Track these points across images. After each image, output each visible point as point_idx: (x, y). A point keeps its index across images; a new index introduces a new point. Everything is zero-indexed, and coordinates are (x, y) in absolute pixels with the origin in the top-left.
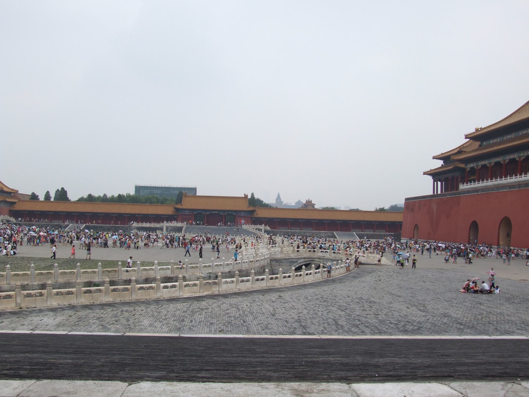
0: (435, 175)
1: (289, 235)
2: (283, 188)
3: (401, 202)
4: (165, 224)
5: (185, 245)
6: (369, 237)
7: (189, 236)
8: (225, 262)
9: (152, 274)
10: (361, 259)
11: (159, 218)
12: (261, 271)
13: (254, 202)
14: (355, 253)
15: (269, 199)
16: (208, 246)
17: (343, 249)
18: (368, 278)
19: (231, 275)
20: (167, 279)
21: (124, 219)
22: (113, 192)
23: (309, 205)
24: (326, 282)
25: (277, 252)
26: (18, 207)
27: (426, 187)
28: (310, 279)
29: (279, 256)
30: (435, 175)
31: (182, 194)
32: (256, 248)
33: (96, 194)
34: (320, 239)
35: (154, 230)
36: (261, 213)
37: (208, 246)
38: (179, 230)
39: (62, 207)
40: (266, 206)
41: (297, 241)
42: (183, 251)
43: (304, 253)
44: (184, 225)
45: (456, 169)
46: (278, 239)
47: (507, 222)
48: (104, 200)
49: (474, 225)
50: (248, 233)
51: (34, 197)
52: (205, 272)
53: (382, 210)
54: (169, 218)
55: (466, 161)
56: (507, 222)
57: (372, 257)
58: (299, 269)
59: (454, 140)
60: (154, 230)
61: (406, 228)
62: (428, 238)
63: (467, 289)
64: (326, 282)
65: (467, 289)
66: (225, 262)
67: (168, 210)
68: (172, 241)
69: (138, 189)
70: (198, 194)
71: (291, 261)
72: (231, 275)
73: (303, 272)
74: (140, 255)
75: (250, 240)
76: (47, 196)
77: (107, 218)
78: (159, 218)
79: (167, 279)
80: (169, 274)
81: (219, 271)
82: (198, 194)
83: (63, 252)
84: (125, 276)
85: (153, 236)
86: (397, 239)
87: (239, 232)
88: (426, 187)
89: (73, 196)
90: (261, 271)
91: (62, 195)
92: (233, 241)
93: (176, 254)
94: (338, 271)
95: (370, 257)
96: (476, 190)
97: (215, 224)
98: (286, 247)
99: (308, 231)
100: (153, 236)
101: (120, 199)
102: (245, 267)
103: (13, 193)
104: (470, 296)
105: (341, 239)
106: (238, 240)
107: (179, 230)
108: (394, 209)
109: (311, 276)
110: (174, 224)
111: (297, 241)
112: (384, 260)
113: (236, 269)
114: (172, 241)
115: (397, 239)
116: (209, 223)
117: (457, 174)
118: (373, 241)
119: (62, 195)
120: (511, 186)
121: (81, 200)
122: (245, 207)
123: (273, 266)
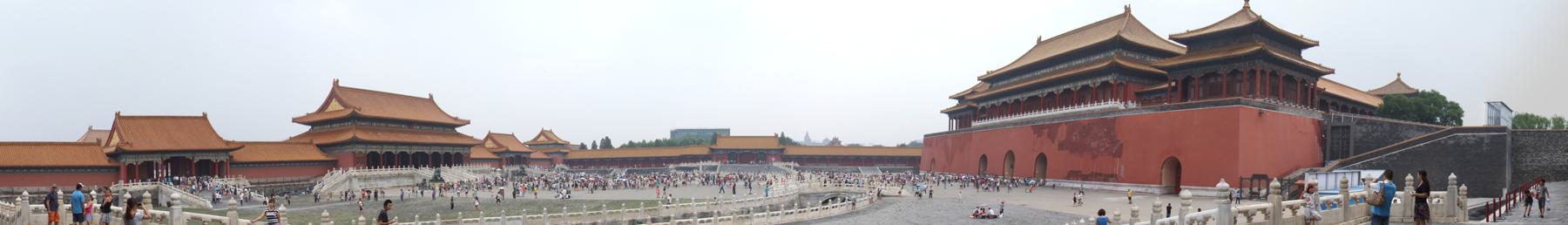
0: (952, 113)
1: (817, 171)
2: (811, 126)
3: (920, 139)
4: (701, 164)
5: (719, 182)
6: (891, 171)
7: (723, 175)
8: (756, 197)
9: (689, 210)
10: (884, 192)
11: (695, 158)
12: (790, 205)
13: (784, 140)
14: (878, 185)
15: (798, 138)
16: (741, 183)
17: (867, 181)
18: (890, 209)
19: (762, 209)
20: (704, 215)
21: (660, 161)
22: (650, 138)
23: (836, 141)
24: (851, 214)
25: (805, 187)
26: (571, 156)
27: (943, 124)
28: (836, 212)
29: (807, 191)
30: (952, 113)
31: (716, 135)
32: (786, 183)
33: (636, 141)
34: (845, 173)
35: (691, 169)
36: (791, 151)
37: (741, 183)
38: (714, 168)
39: (606, 155)
40: (795, 144)
41: (824, 176)
42: (717, 188)
43: (831, 187)
44: (718, 164)
45: (970, 108)
46: (807, 175)
47: (1011, 155)
48: (644, 145)
49: (984, 158)
50: (778, 170)
51: (583, 147)
52: (738, 207)
53: (903, 146)
54: (705, 158)
55: (978, 101)
56: (1011, 155)
57: (893, 190)
58: (826, 202)
59: (968, 81)
60: (691, 169)
61: (925, 162)
62: (944, 170)
63: (976, 216)
64: (851, 214)
65: (976, 216)
66: (756, 197)
67: (704, 151)
68: (707, 179)
69: (673, 133)
70: (732, 134)
71: (818, 195)
72: (762, 209)
73: (830, 205)
74: (676, 193)
75: (780, 176)
76: (594, 145)
77: (646, 162)
78: (695, 158)
79: (704, 215)
80: (705, 209)
81: (751, 206)
82: (732, 134)
83: (610, 195)
84: (664, 213)
85: (690, 175)
86: (916, 172)
87: (770, 169)
88: (943, 124)
89: (616, 144)
90: (790, 205)
91: (606, 143)
92: (764, 178)
93: (712, 191)
94: (862, 203)
95: (891, 190)
96: (986, 127)
97: (747, 162)
98: (813, 182)
99: (834, 167)
100: (690, 175)
101: (658, 144)
102: (775, 202)
103: (565, 145)
104: (978, 221)
105: (866, 173)
106: (769, 176)
107: (714, 168)
108: (914, 145)
109: (837, 209)
110: (710, 163)
111: (824, 176)
112: (904, 192)
113: (767, 204)
114: (707, 179)
115: (916, 172)
116: (741, 162)
117: (970, 112)
118: (895, 175)
119: (606, 143)
120: (1015, 123)
121: (623, 147)
122: (775, 146)
123: (801, 200)
